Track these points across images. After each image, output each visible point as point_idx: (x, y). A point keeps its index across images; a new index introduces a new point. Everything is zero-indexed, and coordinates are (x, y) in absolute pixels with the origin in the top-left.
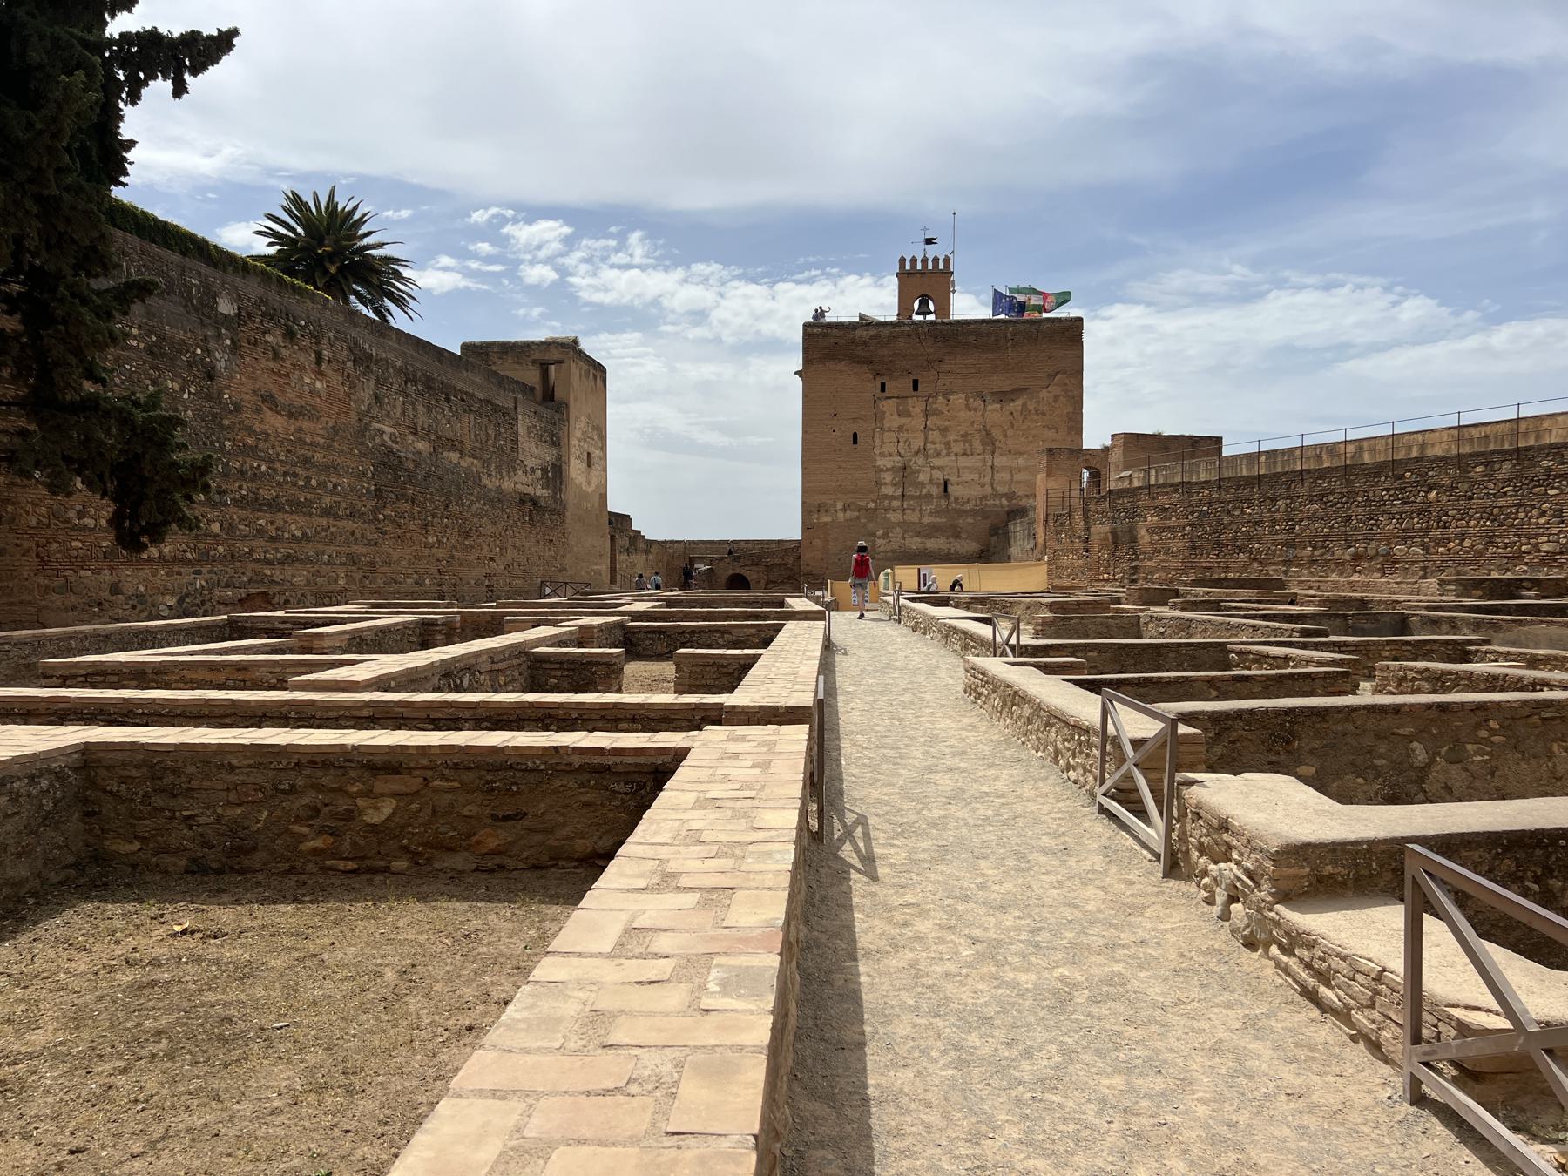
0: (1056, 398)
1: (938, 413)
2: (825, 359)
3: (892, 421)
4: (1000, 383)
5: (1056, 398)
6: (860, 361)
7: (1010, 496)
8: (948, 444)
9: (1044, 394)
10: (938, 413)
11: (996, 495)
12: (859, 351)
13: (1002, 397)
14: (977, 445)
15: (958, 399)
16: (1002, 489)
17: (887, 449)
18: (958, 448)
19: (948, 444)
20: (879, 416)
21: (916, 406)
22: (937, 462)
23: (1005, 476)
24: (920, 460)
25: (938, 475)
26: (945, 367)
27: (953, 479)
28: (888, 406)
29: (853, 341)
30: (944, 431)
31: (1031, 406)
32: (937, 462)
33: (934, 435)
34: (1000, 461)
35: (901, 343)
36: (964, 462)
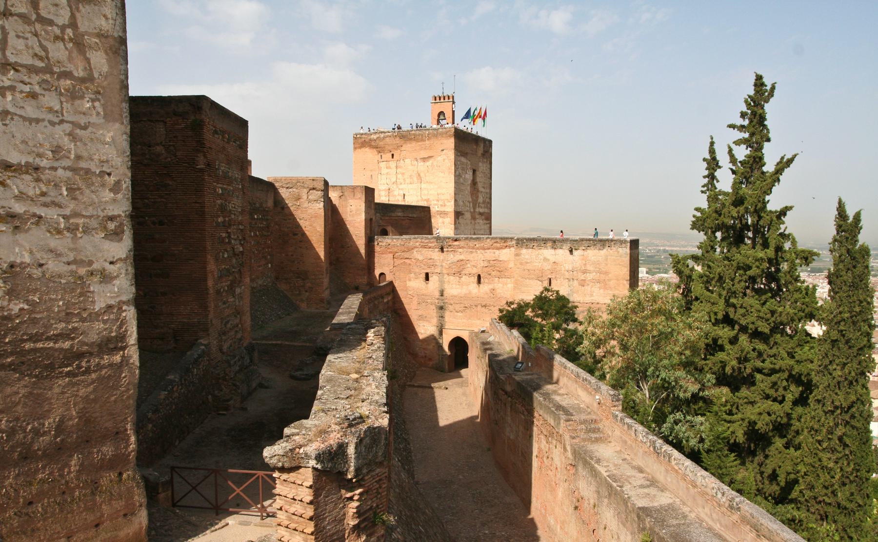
0: (444, 160)
1: (401, 167)
2: (360, 148)
3: (384, 171)
4: (424, 154)
5: (444, 160)
6: (371, 147)
7: (428, 200)
8: (404, 180)
9: (439, 158)
10: (401, 167)
11: (422, 200)
12: (373, 143)
13: (424, 159)
14: (415, 179)
15: (408, 161)
16: (424, 197)
17: (384, 181)
18: (408, 181)
19: (404, 180)
20: (380, 168)
21: (393, 164)
22: (401, 187)
23: (425, 192)
24: (395, 186)
25: (402, 193)
26: (403, 148)
27: (406, 194)
28: (383, 165)
29: (370, 140)
30: (403, 174)
31: (435, 164)
32: (401, 187)
33: (400, 176)
34: (423, 186)
35: (387, 139)
36: (410, 186)
